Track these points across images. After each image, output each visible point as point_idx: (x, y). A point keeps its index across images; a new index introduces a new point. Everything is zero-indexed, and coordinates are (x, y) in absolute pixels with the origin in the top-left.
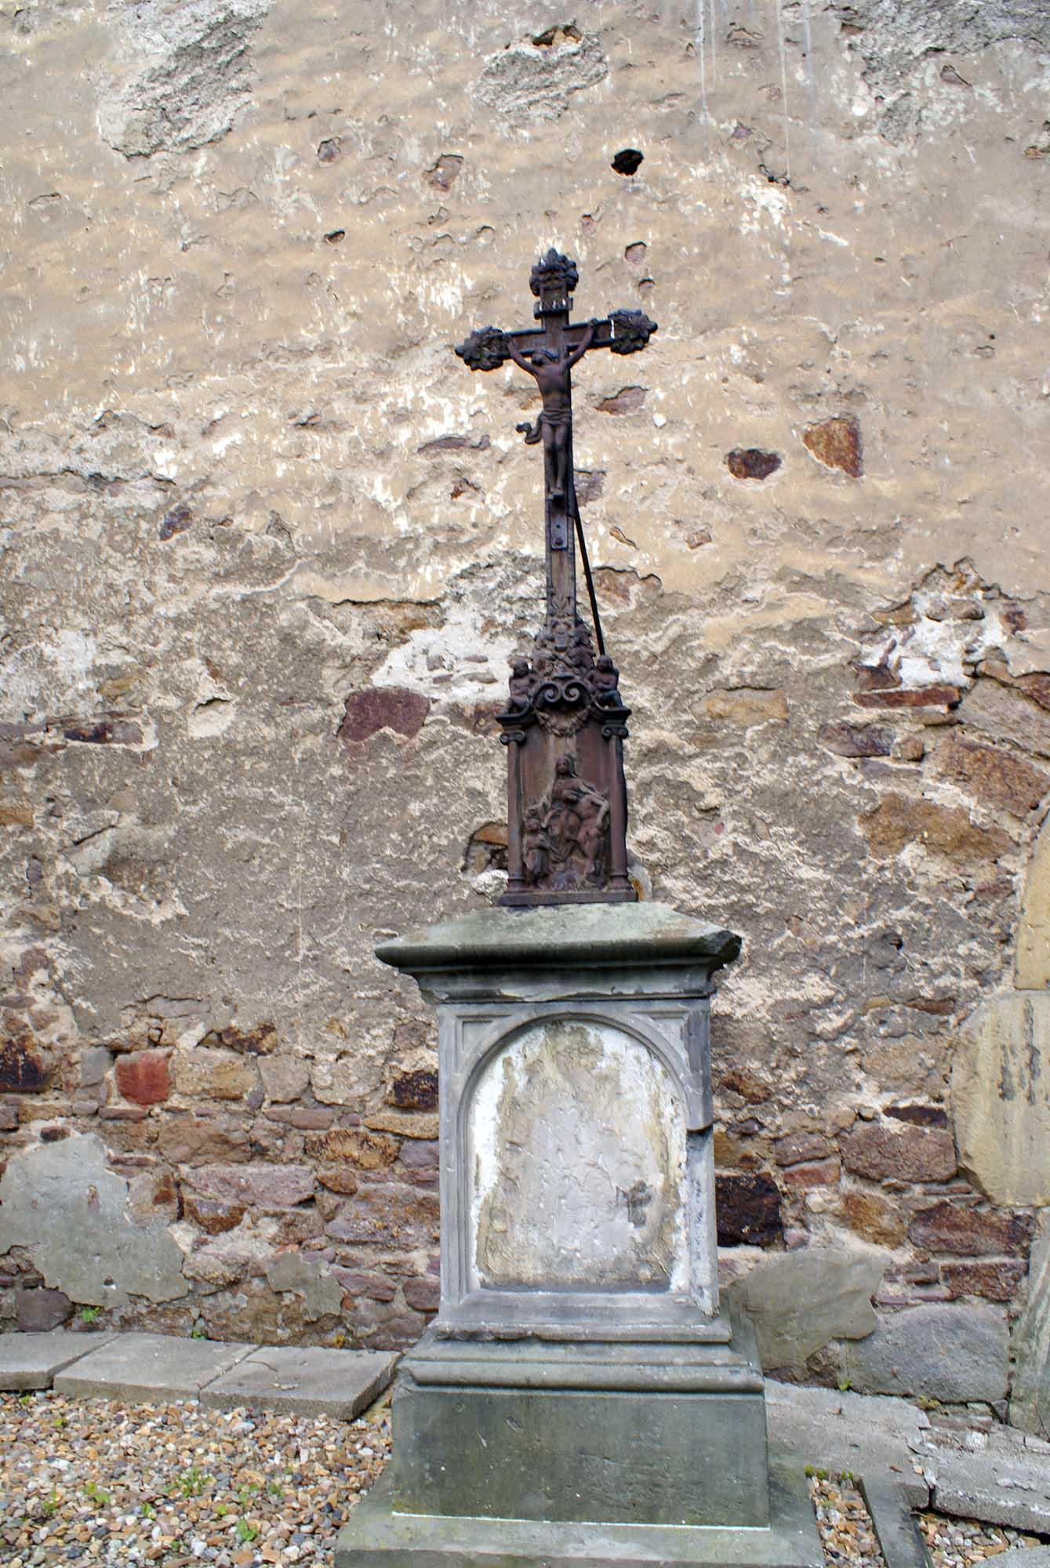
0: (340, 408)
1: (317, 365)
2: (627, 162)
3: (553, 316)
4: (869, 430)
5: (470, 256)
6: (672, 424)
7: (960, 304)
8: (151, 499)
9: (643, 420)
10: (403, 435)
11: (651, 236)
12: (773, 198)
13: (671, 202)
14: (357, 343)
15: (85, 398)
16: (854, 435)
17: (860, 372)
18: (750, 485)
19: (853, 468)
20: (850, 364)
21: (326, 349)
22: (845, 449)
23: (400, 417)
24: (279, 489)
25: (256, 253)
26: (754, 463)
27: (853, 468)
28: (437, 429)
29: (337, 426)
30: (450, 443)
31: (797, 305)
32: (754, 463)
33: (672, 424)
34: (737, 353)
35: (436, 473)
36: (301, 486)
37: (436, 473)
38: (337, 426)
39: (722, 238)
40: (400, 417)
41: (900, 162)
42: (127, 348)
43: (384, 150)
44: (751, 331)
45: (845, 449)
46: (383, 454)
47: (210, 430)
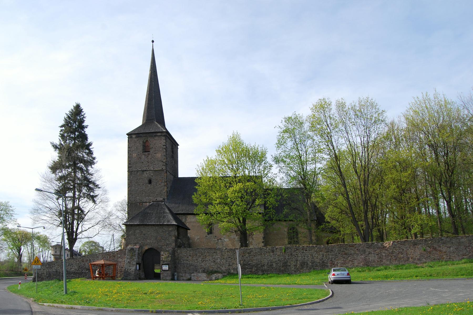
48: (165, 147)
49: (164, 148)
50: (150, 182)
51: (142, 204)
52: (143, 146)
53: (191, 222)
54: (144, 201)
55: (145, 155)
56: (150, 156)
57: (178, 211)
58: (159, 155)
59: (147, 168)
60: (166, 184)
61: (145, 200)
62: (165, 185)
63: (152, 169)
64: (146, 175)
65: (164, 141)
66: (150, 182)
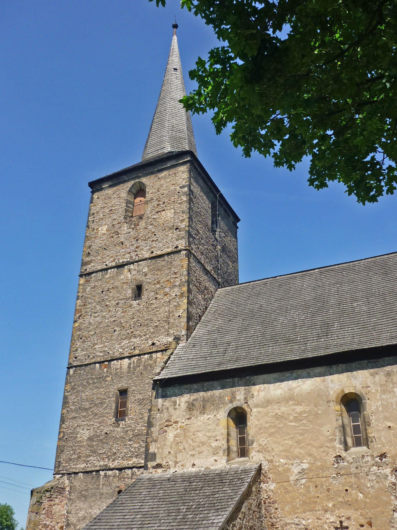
0: (321, 517)
1: (318, 512)
2: (347, 490)
3: (341, 526)
4: (372, 523)
5: (332, 501)
6: (354, 521)
7: (380, 509)
8: (303, 527)
9: (351, 520)
10: (328, 521)
11: (350, 499)
12: (361, 495)
13: (351, 495)
14: (322, 510)
15: (295, 514)
16: (371, 523)
17: (371, 516)
18: (362, 528)
19: (371, 526)
20: (370, 515)
21: (319, 510)
22: (370, 524)
23: (327, 519)
24: (316, 526)
25: (310, 498)
26: (362, 526)
27: (371, 526)
28: (331, 521)
29: (321, 519)
30: (333, 522)
31: (364, 508)
32: (362, 526)
33: (354, 521)
34: (359, 513)
35: (332, 525)
36: (318, 526)
37: (332, 525)
38: (321, 519)
39: (356, 500)
40: (327, 519)
41: (373, 492)
42: (298, 509)
43: (322, 486)
44: (360, 511)
45: (370, 524)
46: (326, 523)
47: (308, 519)
48: (186, 189)
49: (185, 193)
50: (139, 290)
51: (109, 367)
52: (128, 202)
53: (268, 402)
54: (117, 355)
55: (130, 223)
56: (142, 224)
57: (219, 364)
58: (168, 215)
59: (133, 254)
60: (185, 289)
61: (117, 351)
62: (182, 295)
63: (147, 255)
64: (127, 274)
65: (186, 175)
66: (139, 290)
